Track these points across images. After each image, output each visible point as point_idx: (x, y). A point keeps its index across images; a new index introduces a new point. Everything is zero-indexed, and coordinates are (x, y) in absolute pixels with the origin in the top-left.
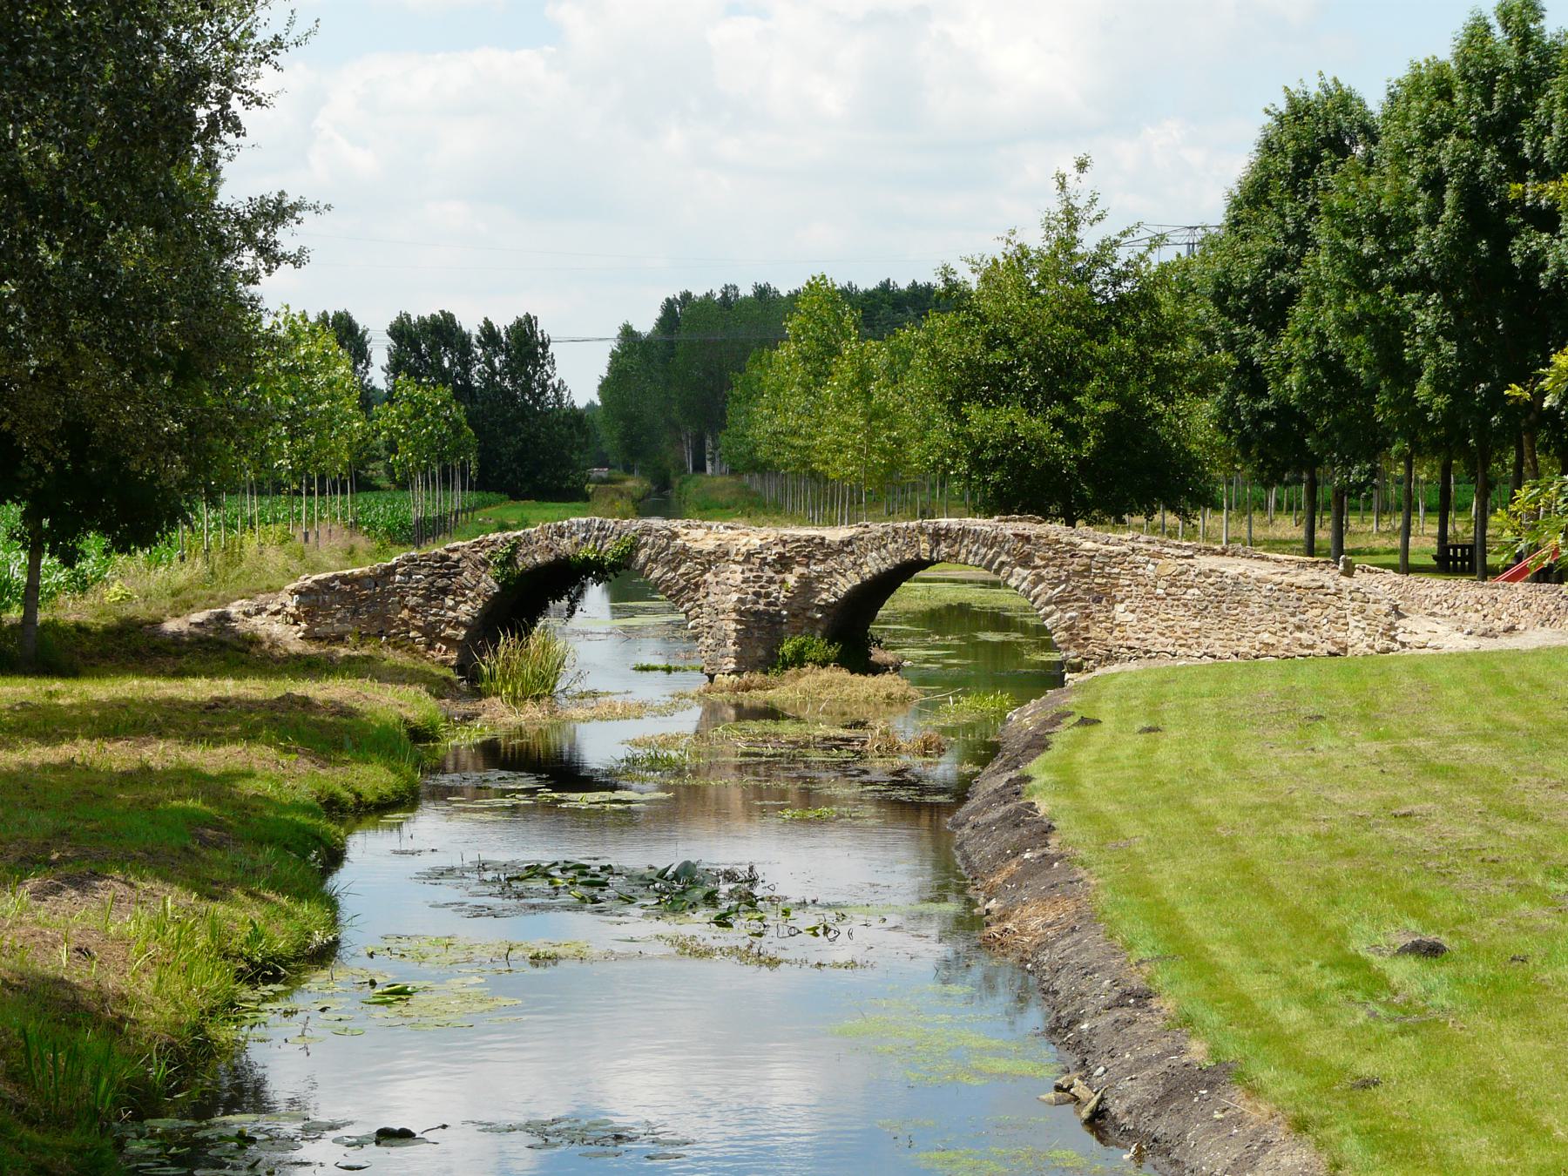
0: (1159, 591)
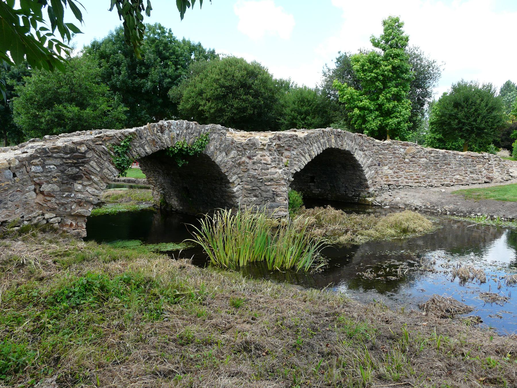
0: (407, 160)
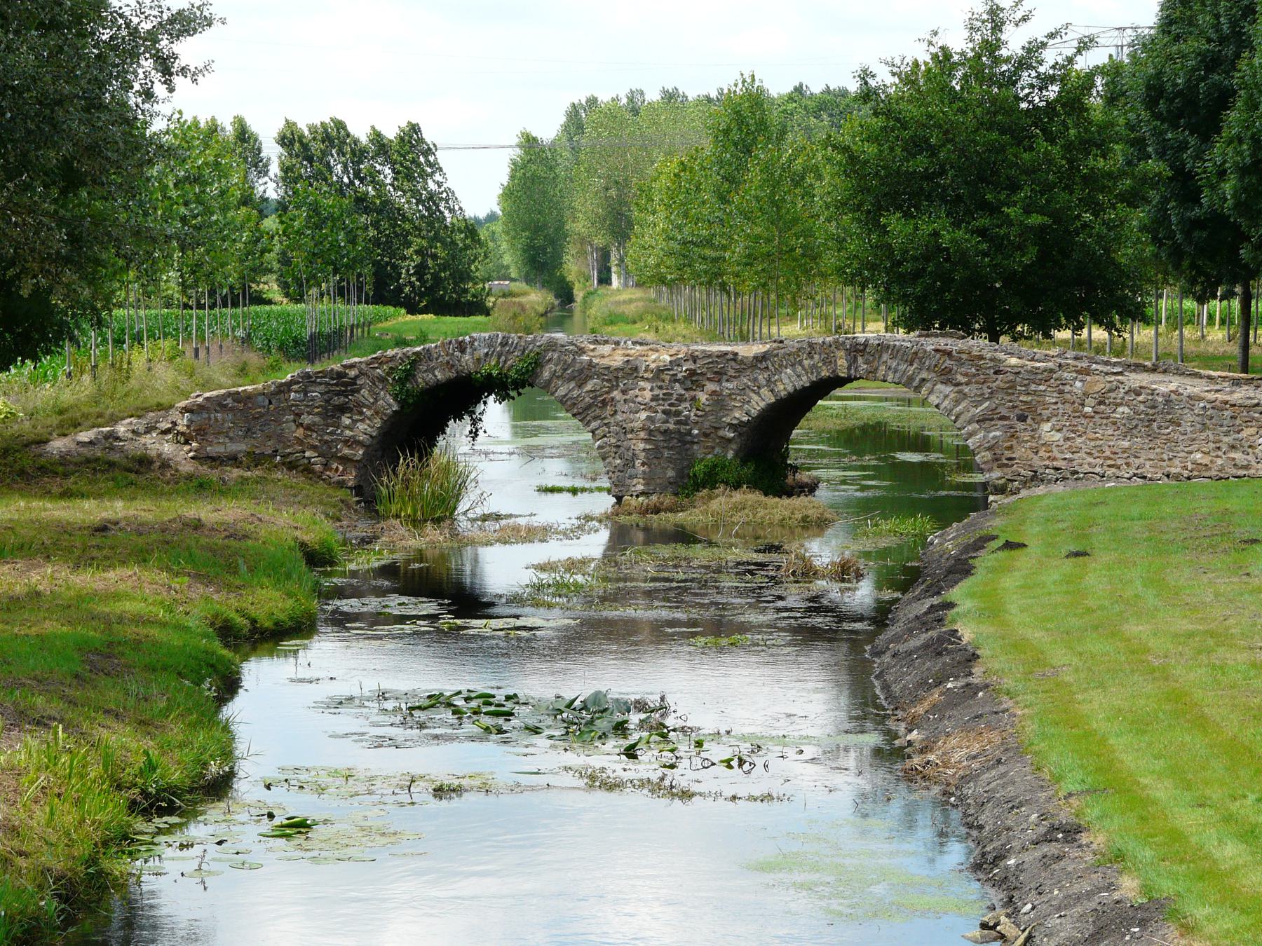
0: (1088, 410)
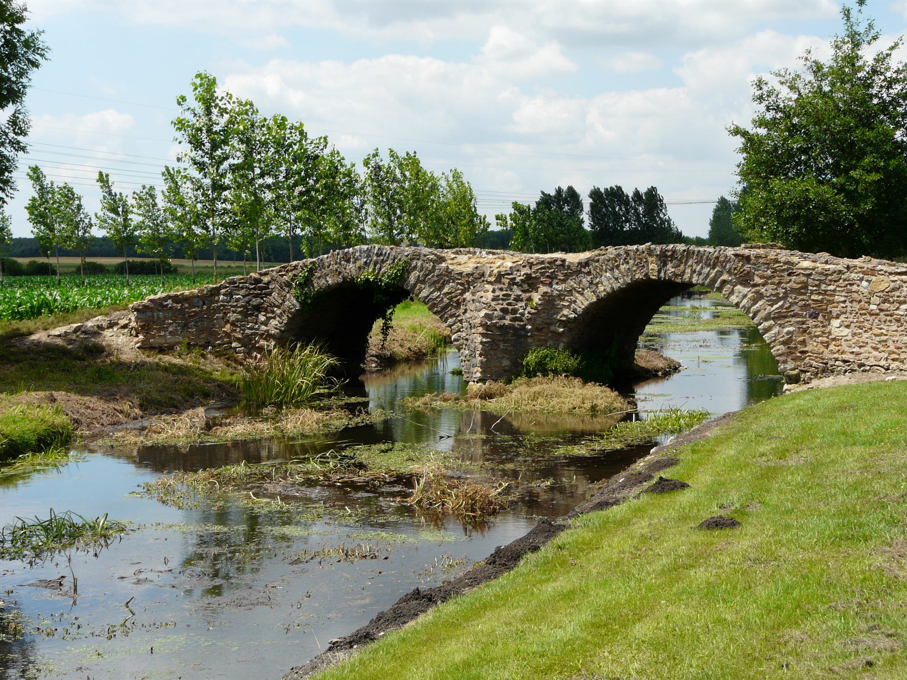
0: (873, 307)
